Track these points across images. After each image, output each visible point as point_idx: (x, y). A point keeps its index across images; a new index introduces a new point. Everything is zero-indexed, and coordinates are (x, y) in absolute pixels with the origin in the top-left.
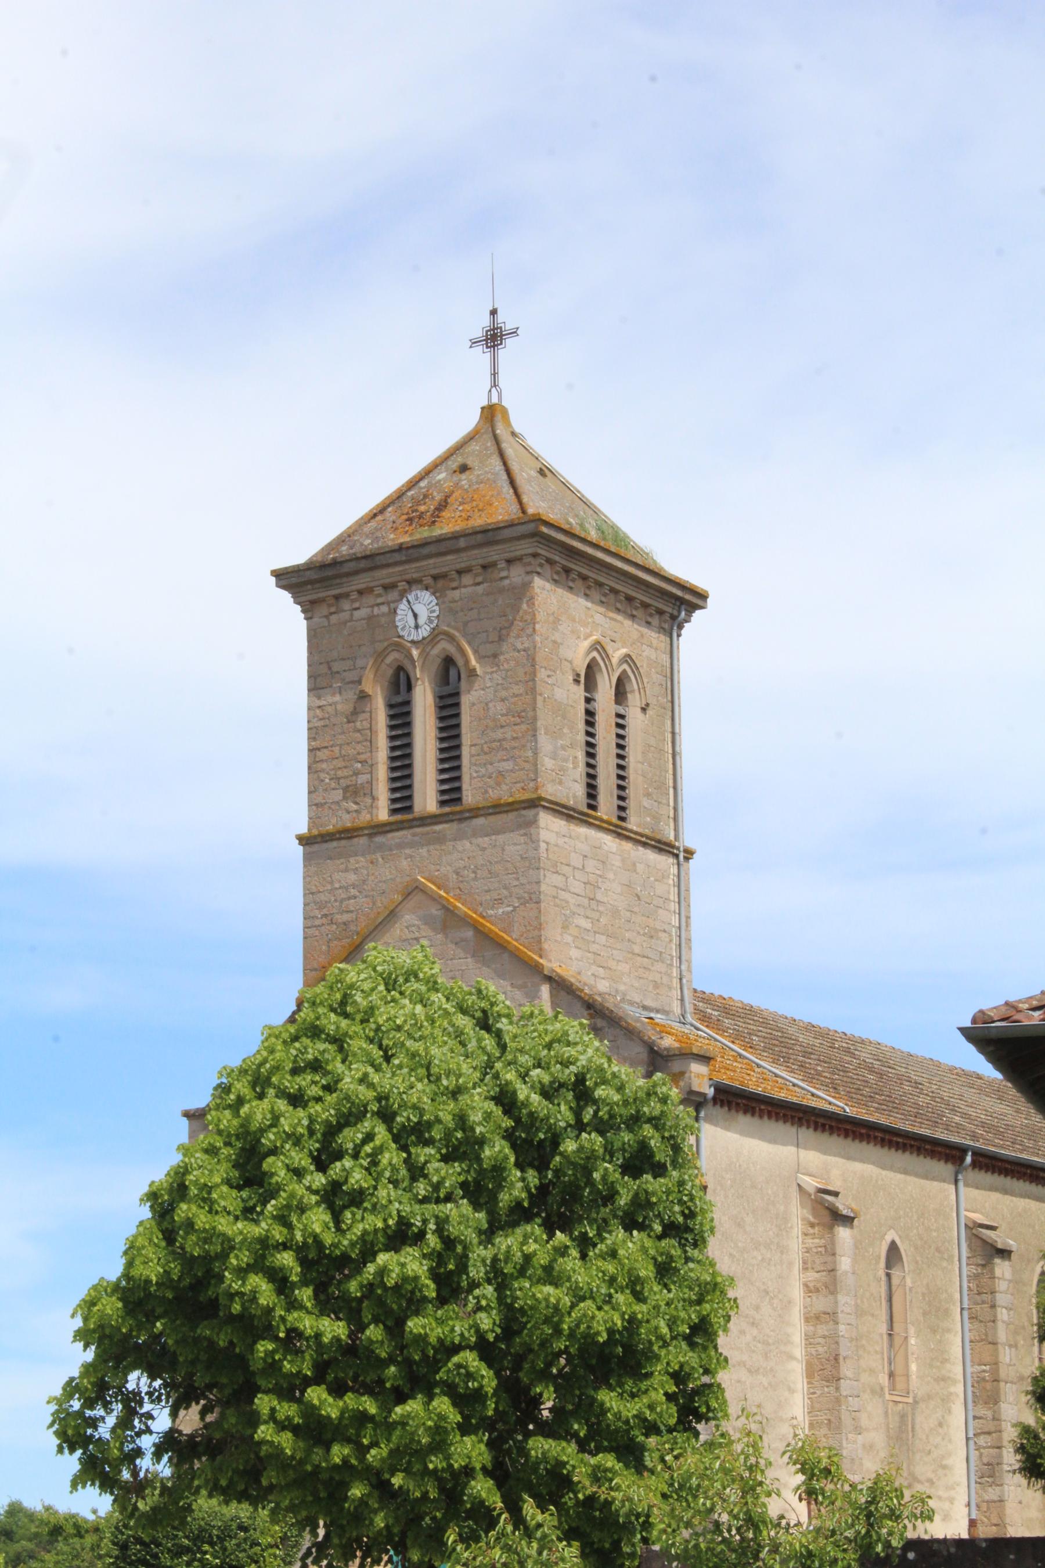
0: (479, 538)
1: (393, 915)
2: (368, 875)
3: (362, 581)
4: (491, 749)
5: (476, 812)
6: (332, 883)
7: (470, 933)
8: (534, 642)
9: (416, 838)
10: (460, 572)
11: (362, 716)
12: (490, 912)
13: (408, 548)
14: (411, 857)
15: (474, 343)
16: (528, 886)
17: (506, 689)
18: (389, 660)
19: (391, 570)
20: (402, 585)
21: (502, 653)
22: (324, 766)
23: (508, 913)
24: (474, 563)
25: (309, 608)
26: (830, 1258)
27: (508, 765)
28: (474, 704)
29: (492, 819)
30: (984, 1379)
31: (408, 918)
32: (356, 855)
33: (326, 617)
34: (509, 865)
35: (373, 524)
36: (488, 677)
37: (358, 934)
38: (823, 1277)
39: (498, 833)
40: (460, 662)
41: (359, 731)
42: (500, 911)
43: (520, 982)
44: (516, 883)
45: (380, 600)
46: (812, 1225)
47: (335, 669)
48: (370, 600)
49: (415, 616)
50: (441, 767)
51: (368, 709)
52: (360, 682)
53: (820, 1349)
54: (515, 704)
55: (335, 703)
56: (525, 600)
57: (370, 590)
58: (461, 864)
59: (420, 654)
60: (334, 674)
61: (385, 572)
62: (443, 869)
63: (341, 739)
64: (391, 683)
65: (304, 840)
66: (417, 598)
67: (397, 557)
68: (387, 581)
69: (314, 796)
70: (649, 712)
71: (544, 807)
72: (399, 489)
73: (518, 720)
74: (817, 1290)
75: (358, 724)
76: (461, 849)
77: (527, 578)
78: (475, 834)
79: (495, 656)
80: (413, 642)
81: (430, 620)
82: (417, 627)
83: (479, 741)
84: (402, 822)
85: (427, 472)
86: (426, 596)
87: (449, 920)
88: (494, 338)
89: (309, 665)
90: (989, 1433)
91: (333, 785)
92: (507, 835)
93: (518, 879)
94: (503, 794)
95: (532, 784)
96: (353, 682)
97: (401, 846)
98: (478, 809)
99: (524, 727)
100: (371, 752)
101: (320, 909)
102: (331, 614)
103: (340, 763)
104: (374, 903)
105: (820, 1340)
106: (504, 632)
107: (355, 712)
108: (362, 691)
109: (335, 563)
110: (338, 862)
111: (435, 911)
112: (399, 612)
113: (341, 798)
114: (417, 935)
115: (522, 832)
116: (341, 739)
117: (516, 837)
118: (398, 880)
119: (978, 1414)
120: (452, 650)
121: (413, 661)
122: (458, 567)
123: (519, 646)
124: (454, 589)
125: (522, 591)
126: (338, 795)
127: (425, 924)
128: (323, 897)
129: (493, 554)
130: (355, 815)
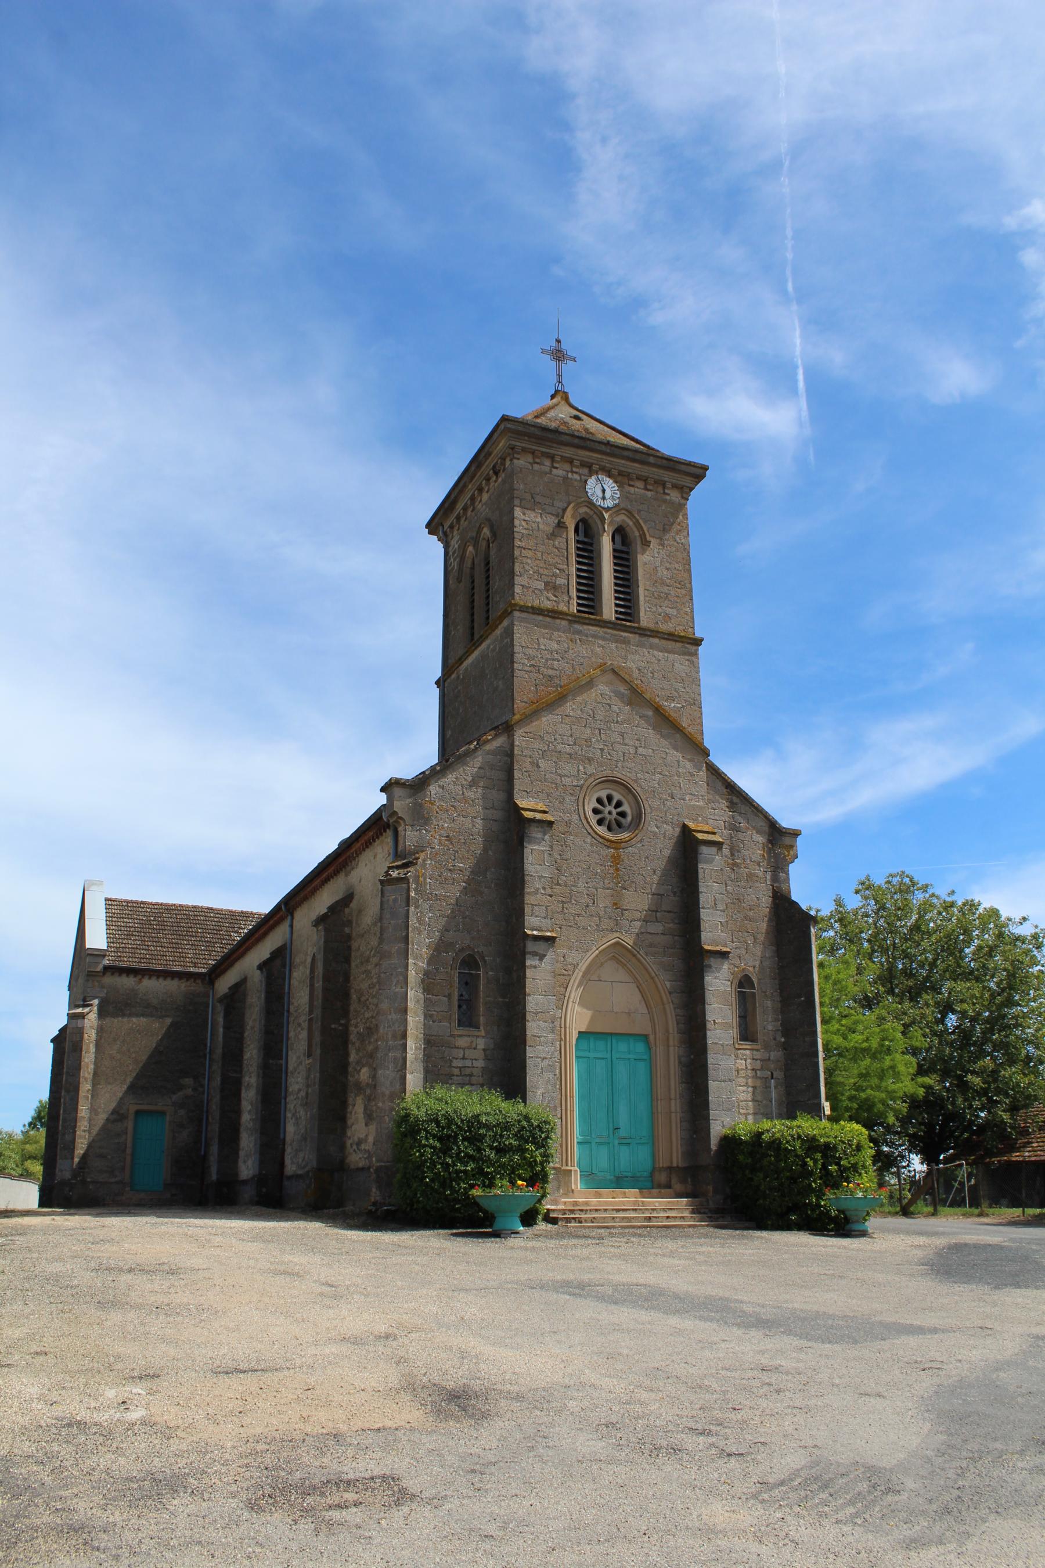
1: (590, 684)
3: (568, 452)
4: (659, 597)
5: (645, 633)
7: (650, 713)
13: (612, 446)
19: (591, 454)
22: (529, 561)
27: (674, 612)
29: (664, 642)
31: (602, 688)
32: (558, 630)
39: (669, 652)
48: (567, 467)
49: (604, 491)
51: (564, 536)
67: (603, 448)
82: (604, 498)
97: (593, 636)
98: (658, 632)
99: (683, 592)
101: (528, 659)
107: (553, 536)
111: (622, 689)
116: (542, 548)
118: (593, 659)
124: (630, 485)
126: (541, 585)
128: (530, 651)
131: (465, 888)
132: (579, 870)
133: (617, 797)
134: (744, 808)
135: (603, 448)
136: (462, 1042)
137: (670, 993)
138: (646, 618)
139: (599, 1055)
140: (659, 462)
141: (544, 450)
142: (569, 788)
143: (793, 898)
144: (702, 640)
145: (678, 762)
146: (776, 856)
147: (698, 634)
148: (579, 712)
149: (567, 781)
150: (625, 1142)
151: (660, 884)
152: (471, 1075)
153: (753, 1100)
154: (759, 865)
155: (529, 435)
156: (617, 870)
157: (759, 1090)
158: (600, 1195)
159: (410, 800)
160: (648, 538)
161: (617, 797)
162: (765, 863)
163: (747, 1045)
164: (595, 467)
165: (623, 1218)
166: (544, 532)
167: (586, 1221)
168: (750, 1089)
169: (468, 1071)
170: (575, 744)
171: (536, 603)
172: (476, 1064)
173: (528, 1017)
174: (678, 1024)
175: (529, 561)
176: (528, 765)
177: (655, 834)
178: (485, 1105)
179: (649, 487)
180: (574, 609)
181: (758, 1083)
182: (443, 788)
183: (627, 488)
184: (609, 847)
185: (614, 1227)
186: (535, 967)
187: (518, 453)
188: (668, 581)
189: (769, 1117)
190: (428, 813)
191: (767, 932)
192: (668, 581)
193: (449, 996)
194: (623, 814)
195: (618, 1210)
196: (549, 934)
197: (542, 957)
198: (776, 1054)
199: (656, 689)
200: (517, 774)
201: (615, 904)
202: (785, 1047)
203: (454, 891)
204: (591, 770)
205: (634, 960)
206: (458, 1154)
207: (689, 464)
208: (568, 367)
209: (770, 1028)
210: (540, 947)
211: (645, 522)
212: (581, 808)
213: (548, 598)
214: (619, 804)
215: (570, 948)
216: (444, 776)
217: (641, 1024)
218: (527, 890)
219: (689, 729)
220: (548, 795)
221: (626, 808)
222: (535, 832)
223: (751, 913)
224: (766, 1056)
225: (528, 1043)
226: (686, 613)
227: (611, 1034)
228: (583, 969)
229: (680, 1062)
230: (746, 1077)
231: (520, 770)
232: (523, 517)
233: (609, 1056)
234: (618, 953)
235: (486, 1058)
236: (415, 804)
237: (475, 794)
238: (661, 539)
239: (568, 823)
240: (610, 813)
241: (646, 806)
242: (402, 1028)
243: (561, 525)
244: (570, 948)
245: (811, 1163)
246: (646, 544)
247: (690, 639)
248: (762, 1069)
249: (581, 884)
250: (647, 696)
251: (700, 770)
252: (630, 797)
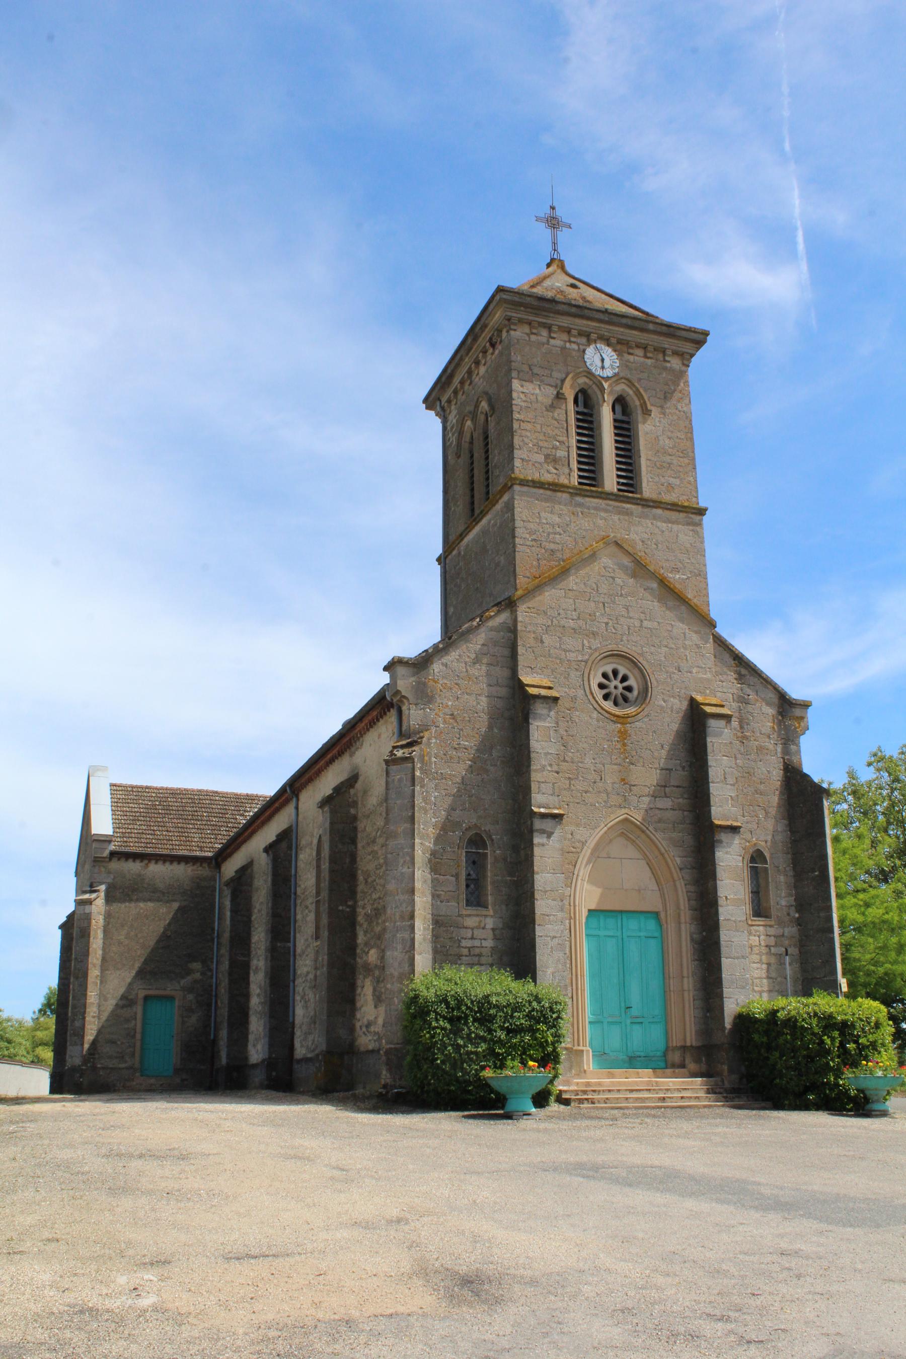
0: (664, 329)
1: (593, 556)
2: (570, 521)
3: (565, 321)
4: (662, 467)
5: (647, 503)
6: (540, 518)
7: (655, 585)
9: (608, 508)
11: (557, 411)
12: (670, 575)
19: (589, 323)
22: (529, 434)
27: (677, 482)
28: (647, 433)
29: (668, 513)
32: (560, 503)
37: (564, 561)
39: (673, 523)
41: (556, 420)
43: (695, 629)
48: (565, 337)
49: (603, 360)
51: (563, 407)
56: (682, 381)
59: (609, 386)
60: (534, 375)
61: (585, 322)
67: (601, 316)
78: (655, 518)
81: (612, 367)
82: (603, 368)
91: (536, 450)
95: (694, 499)
97: (596, 509)
98: (661, 502)
99: (686, 461)
100: (568, 437)
101: (530, 534)
107: (552, 407)
111: (626, 561)
113: (543, 460)
114: (612, 575)
115: (691, 528)
118: (596, 532)
121: (602, 389)
123: (679, 407)
124: (629, 354)
126: (541, 458)
128: (532, 526)
129: (667, 343)
130: (555, 476)
131: (471, 766)
132: (585, 745)
133: (622, 671)
134: (753, 680)
135: (601, 316)
136: (470, 922)
137: (681, 869)
138: (648, 488)
139: (611, 933)
140: (659, 329)
141: (540, 320)
142: (573, 663)
143: (806, 770)
144: (706, 510)
145: (684, 634)
146: (787, 729)
147: (702, 504)
148: (583, 586)
149: (572, 656)
150: (637, 1021)
151: (669, 757)
152: (480, 955)
153: (768, 977)
154: (769, 737)
155: (526, 306)
156: (624, 745)
157: (773, 967)
158: (612, 1076)
159: (413, 679)
160: (649, 407)
161: (622, 671)
162: (775, 736)
163: (760, 921)
164: (593, 336)
165: (637, 1099)
166: (542, 403)
167: (599, 1102)
168: (765, 966)
169: (477, 951)
170: (579, 618)
171: (536, 477)
172: (485, 944)
173: (536, 896)
174: (689, 900)
175: (529, 434)
176: (532, 642)
177: (662, 707)
178: (495, 985)
179: (649, 355)
180: (575, 481)
181: (773, 960)
182: (446, 665)
183: (626, 355)
184: (615, 722)
185: (627, 1108)
186: (543, 845)
187: (515, 324)
188: (670, 450)
189: (784, 994)
190: (432, 691)
191: (779, 806)
192: (670, 450)
193: (457, 876)
194: (629, 689)
195: (632, 1091)
196: (556, 811)
197: (550, 835)
198: (791, 930)
199: (660, 560)
200: (520, 650)
201: (623, 780)
202: (799, 922)
203: (460, 770)
204: (596, 644)
205: (643, 836)
206: (469, 1035)
207: (689, 330)
208: (563, 235)
209: (783, 903)
210: (547, 824)
211: (645, 390)
212: (586, 683)
213: (548, 471)
214: (624, 679)
215: (578, 825)
216: (446, 654)
217: (653, 902)
218: (533, 767)
219: (695, 601)
220: (553, 671)
221: (631, 682)
222: (540, 708)
223: (762, 787)
224: (780, 931)
225: (537, 922)
226: (689, 483)
227: (621, 912)
228: (592, 845)
229: (692, 940)
230: (760, 954)
231: (524, 646)
232: (521, 389)
233: (619, 933)
234: (627, 830)
235: (495, 938)
236: (419, 683)
237: (479, 671)
238: (662, 407)
239: (574, 699)
240: (616, 687)
241: (653, 680)
242: (409, 909)
243: (559, 396)
244: (578, 825)
245: (828, 1041)
246: (647, 412)
247: (694, 508)
248: (776, 945)
249: (588, 761)
250: (651, 568)
251: (707, 642)
252: (636, 671)
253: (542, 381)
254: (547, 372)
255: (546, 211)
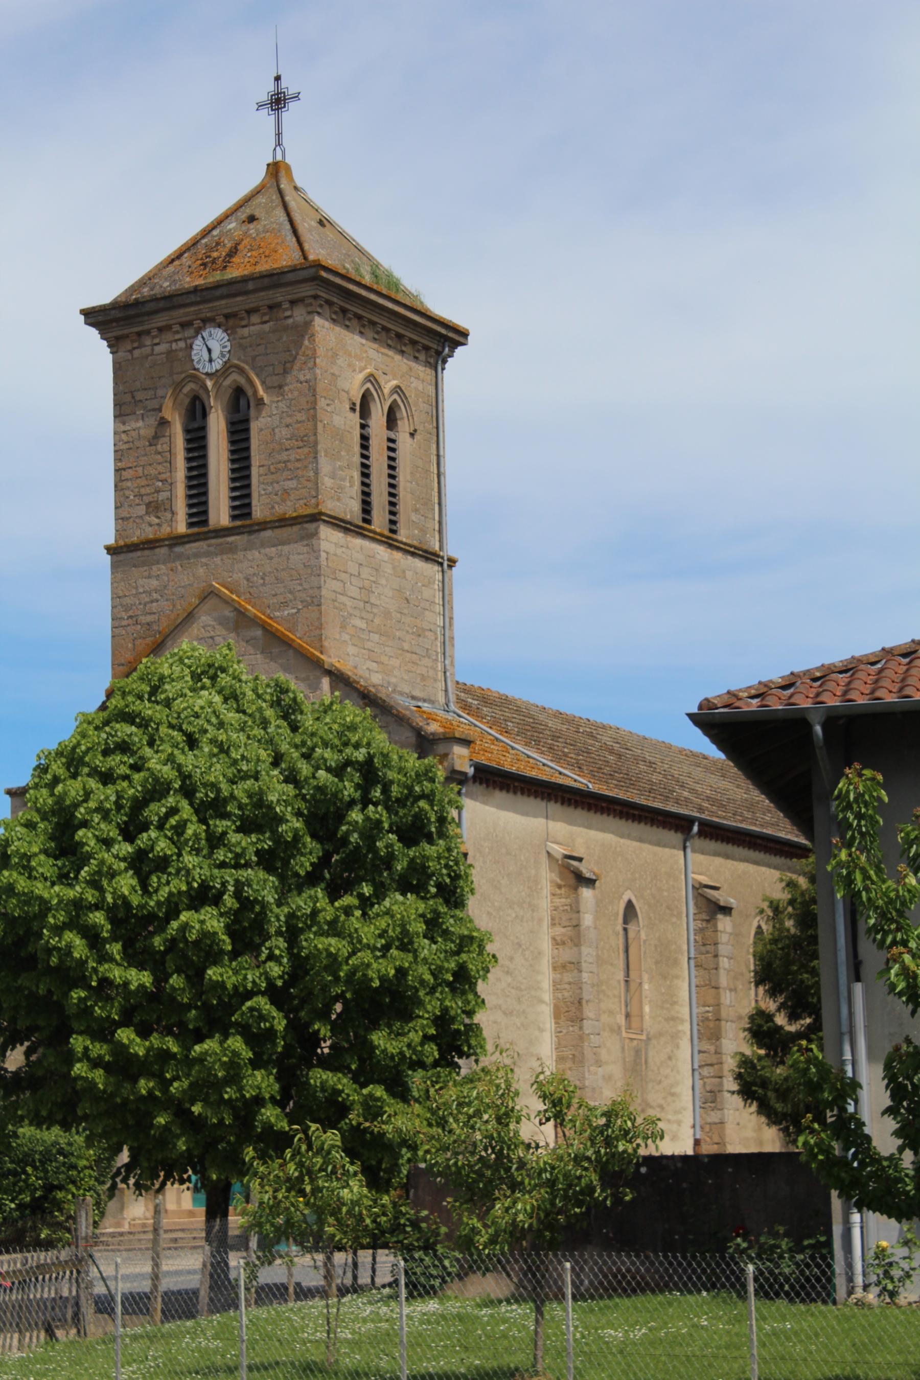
1: (190, 617)
3: (161, 320)
5: (264, 526)
6: (137, 588)
7: (259, 633)
8: (315, 374)
9: (212, 549)
10: (249, 312)
11: (162, 440)
12: (277, 614)
13: (202, 290)
14: (206, 565)
15: (260, 106)
16: (311, 591)
17: (290, 416)
18: (186, 390)
20: (197, 323)
21: (286, 385)
22: (129, 484)
23: (293, 614)
24: (261, 303)
25: (114, 344)
26: (575, 916)
27: (292, 484)
28: (261, 430)
30: (707, 1019)
31: (203, 618)
32: (158, 563)
33: (131, 351)
34: (294, 572)
35: (171, 268)
36: (274, 405)
37: (160, 633)
38: (569, 931)
39: (283, 543)
40: (250, 393)
41: (159, 453)
42: (286, 613)
43: (303, 676)
44: (299, 588)
45: (177, 337)
46: (560, 887)
47: (137, 398)
48: (168, 336)
49: (209, 351)
50: (232, 485)
52: (160, 410)
53: (566, 994)
54: (298, 429)
55: (139, 428)
57: (168, 328)
58: (251, 571)
59: (214, 385)
60: (137, 403)
61: (181, 311)
62: (235, 576)
63: (143, 460)
64: (187, 410)
65: (110, 550)
66: (211, 335)
67: (193, 298)
68: (184, 319)
69: (120, 511)
70: (417, 437)
71: (324, 521)
72: (194, 237)
73: (301, 444)
74: (563, 943)
75: (159, 447)
76: (250, 558)
77: (308, 318)
78: (263, 545)
79: (280, 387)
80: (207, 374)
81: (222, 355)
82: (211, 361)
83: (266, 463)
84: (198, 534)
85: (219, 222)
86: (219, 333)
87: (241, 621)
88: (278, 102)
89: (115, 395)
90: (712, 1065)
91: (137, 501)
92: (292, 546)
93: (301, 585)
94: (288, 509)
95: (313, 501)
96: (154, 410)
97: (197, 555)
98: (265, 522)
99: (306, 450)
101: (126, 611)
102: (134, 348)
103: (143, 482)
104: (174, 606)
105: (567, 986)
106: (288, 365)
107: (156, 437)
108: (162, 418)
109: (137, 303)
110: (142, 569)
111: (228, 613)
112: (194, 347)
114: (212, 634)
115: (305, 542)
116: (143, 460)
117: (300, 547)
118: (195, 585)
119: (703, 1049)
120: (242, 381)
121: (207, 391)
122: (247, 307)
123: (302, 378)
125: (304, 329)
126: (142, 510)
127: (220, 624)
128: (128, 601)
129: (278, 296)
135: (193, 298)
155: (116, 320)
160: (261, 392)
164: (197, 323)
188: (288, 444)
253: (145, 408)
254: (150, 393)
255: (266, 89)
